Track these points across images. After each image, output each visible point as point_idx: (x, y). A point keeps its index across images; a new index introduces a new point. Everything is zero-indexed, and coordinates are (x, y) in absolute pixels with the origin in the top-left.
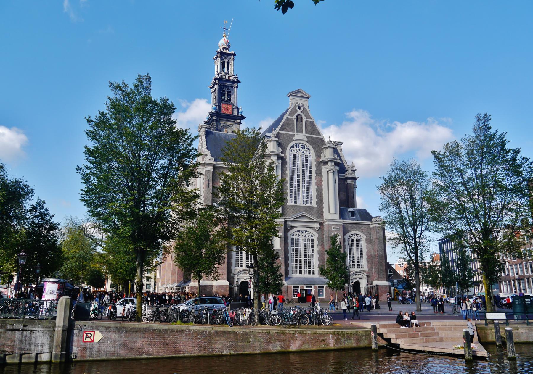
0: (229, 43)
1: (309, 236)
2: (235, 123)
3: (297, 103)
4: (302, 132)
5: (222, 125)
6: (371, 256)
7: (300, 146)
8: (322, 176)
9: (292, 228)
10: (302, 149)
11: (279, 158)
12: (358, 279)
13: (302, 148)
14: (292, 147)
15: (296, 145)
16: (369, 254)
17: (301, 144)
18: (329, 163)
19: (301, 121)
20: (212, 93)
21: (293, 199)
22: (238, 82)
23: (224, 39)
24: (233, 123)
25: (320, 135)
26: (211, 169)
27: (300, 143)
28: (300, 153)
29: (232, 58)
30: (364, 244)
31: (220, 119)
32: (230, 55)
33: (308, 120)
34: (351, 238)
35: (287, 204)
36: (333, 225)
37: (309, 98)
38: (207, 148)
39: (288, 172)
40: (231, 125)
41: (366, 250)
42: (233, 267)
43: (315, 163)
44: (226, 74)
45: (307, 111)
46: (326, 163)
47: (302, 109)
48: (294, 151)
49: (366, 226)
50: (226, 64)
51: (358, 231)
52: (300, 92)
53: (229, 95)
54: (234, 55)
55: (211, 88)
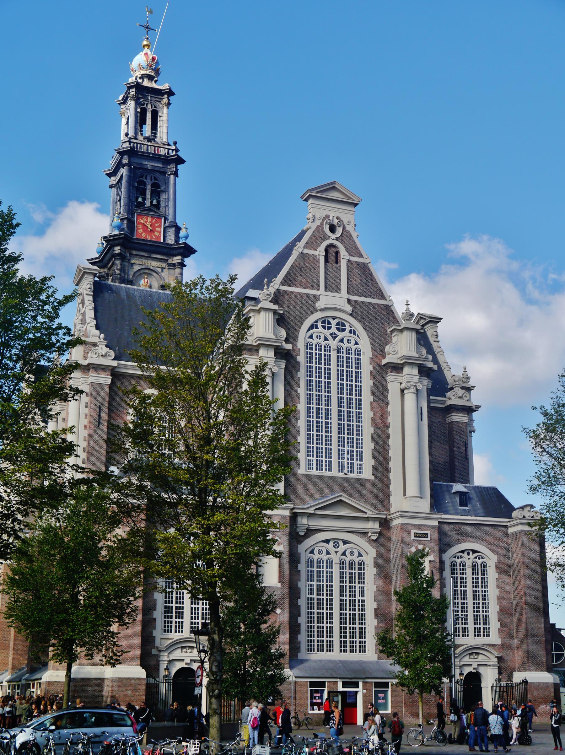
0: (157, 63)
1: (352, 553)
2: (169, 265)
3: (328, 216)
4: (338, 289)
5: (136, 268)
6: (510, 606)
7: (334, 326)
8: (387, 402)
9: (310, 532)
10: (337, 332)
11: (279, 353)
12: (475, 665)
13: (338, 329)
15: (323, 322)
16: (505, 602)
17: (337, 321)
18: (406, 370)
19: (337, 261)
21: (314, 458)
22: (180, 161)
23: (146, 54)
24: (164, 265)
25: (385, 299)
26: (107, 379)
27: (334, 318)
28: (334, 343)
29: (165, 100)
30: (492, 575)
31: (131, 254)
32: (159, 93)
33: (353, 259)
34: (458, 561)
35: (299, 472)
36: (413, 526)
37: (356, 205)
38: (97, 328)
39: (302, 390)
40: (160, 270)
41: (497, 592)
42: (158, 633)
43: (371, 368)
44: (148, 139)
45: (350, 236)
46: (397, 368)
47: (339, 231)
48: (319, 337)
49: (498, 529)
50: (149, 116)
51: (477, 542)
52: (334, 188)
53: (157, 192)
54: (170, 93)
55: (109, 175)
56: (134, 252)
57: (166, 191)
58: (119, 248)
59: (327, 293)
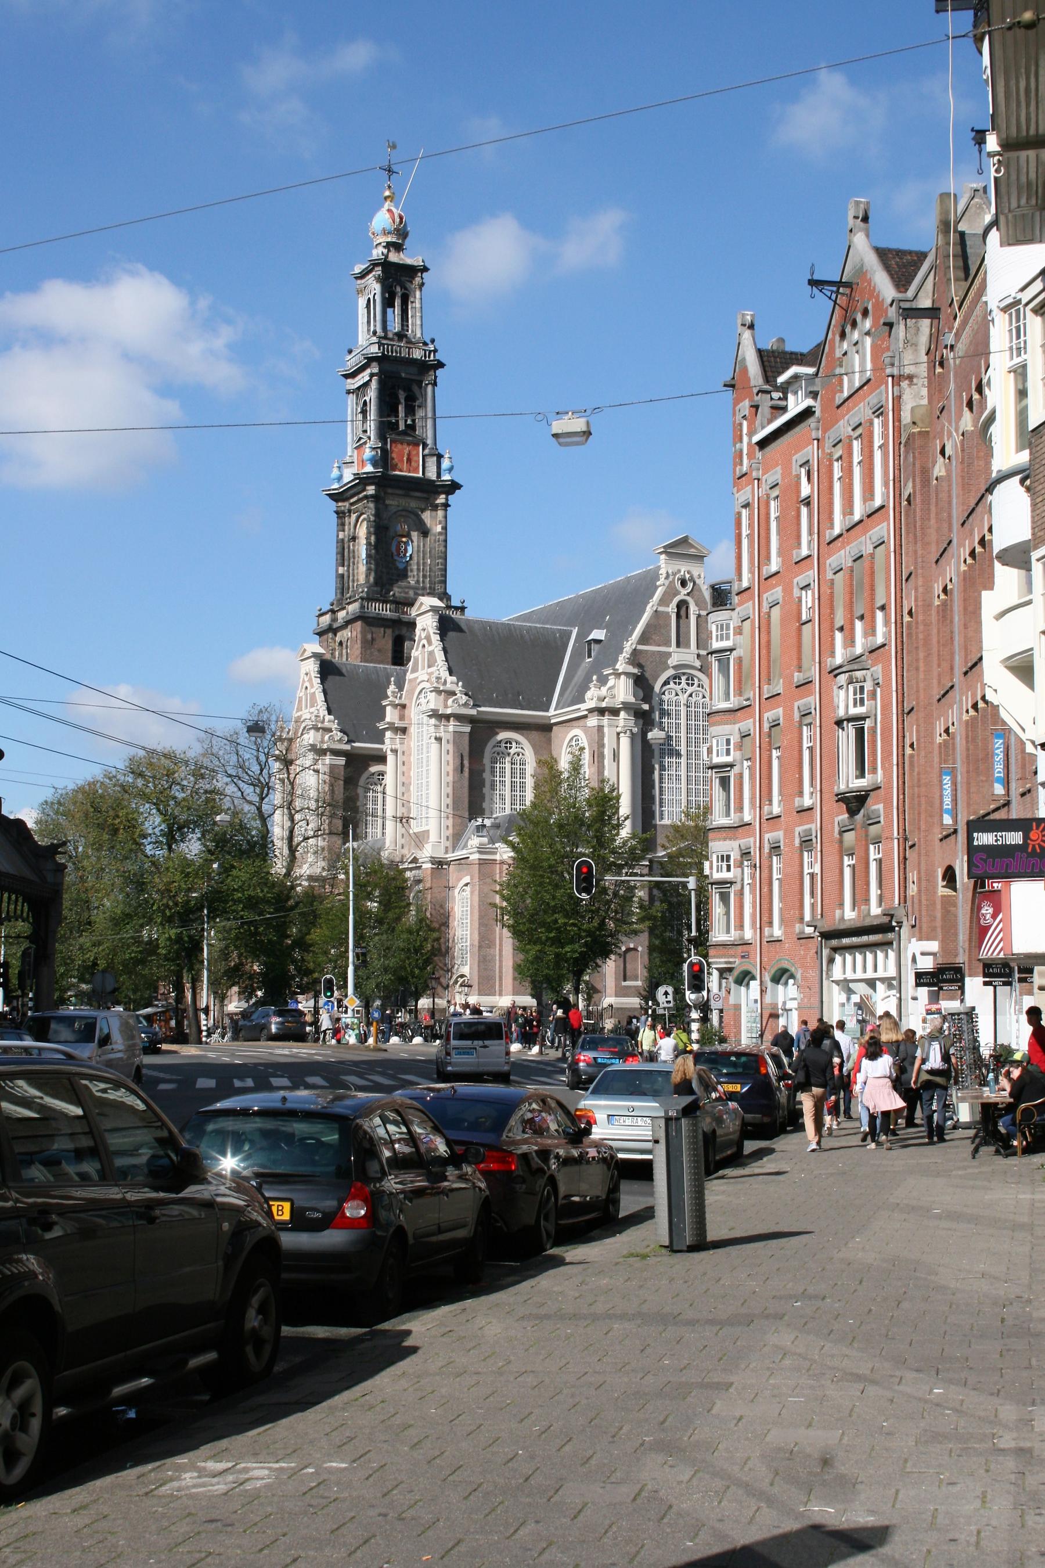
4: (688, 645)
14: (666, 683)
20: (349, 392)
22: (440, 365)
23: (389, 211)
27: (684, 674)
28: (683, 698)
29: (418, 280)
44: (401, 336)
45: (700, 590)
47: (690, 585)
56: (390, 491)
57: (423, 406)
58: (373, 487)
59: (679, 650)
